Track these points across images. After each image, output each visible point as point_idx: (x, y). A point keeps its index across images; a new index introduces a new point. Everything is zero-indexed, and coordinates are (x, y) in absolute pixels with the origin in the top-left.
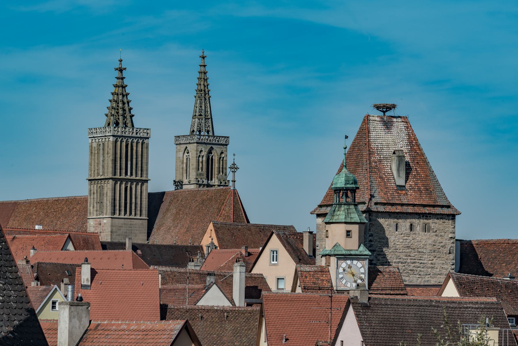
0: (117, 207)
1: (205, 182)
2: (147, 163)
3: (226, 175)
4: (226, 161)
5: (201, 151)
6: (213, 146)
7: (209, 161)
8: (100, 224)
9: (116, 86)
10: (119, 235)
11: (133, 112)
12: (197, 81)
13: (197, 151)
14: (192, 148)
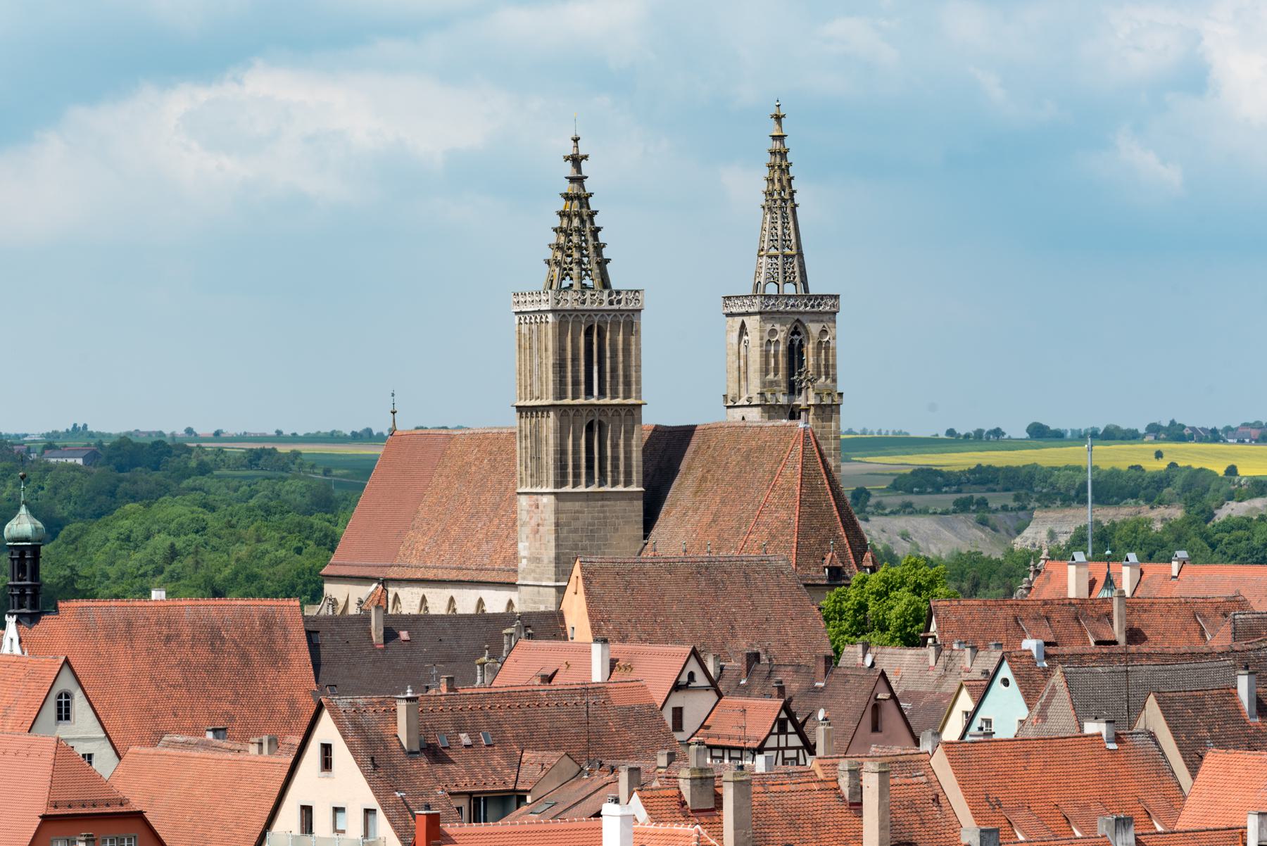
0: (570, 470)
1: (783, 400)
2: (639, 366)
3: (834, 380)
4: (834, 349)
5: (773, 332)
6: (800, 317)
7: (794, 354)
8: (537, 507)
9: (567, 197)
10: (576, 531)
11: (606, 253)
12: (766, 172)
13: (761, 331)
14: (753, 323)
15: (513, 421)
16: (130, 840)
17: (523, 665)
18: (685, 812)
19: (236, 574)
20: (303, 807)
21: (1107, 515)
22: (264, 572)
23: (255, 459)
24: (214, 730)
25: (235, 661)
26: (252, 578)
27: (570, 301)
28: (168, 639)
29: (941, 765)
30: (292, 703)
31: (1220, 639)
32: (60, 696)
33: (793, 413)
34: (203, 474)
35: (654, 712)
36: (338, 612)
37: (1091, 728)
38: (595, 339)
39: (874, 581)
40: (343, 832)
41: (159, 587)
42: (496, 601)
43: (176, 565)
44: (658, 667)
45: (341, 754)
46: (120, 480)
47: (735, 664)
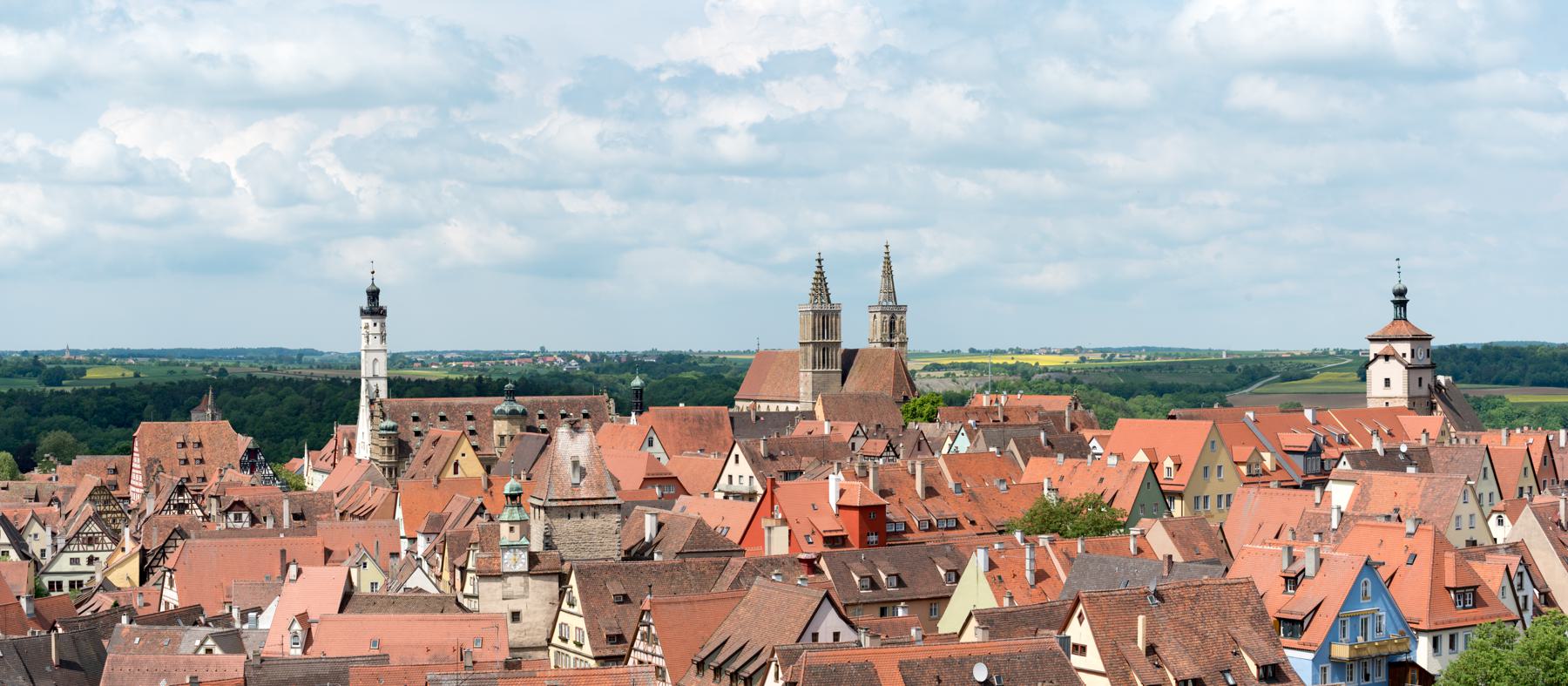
7: (892, 325)
15: (798, 347)
17: (801, 429)
18: (857, 478)
21: (996, 379)
23: (712, 359)
27: (817, 307)
29: (941, 462)
31: (1034, 420)
33: (892, 345)
35: (846, 444)
37: (992, 449)
38: (825, 320)
39: (919, 401)
42: (792, 407)
44: (847, 429)
47: (872, 428)
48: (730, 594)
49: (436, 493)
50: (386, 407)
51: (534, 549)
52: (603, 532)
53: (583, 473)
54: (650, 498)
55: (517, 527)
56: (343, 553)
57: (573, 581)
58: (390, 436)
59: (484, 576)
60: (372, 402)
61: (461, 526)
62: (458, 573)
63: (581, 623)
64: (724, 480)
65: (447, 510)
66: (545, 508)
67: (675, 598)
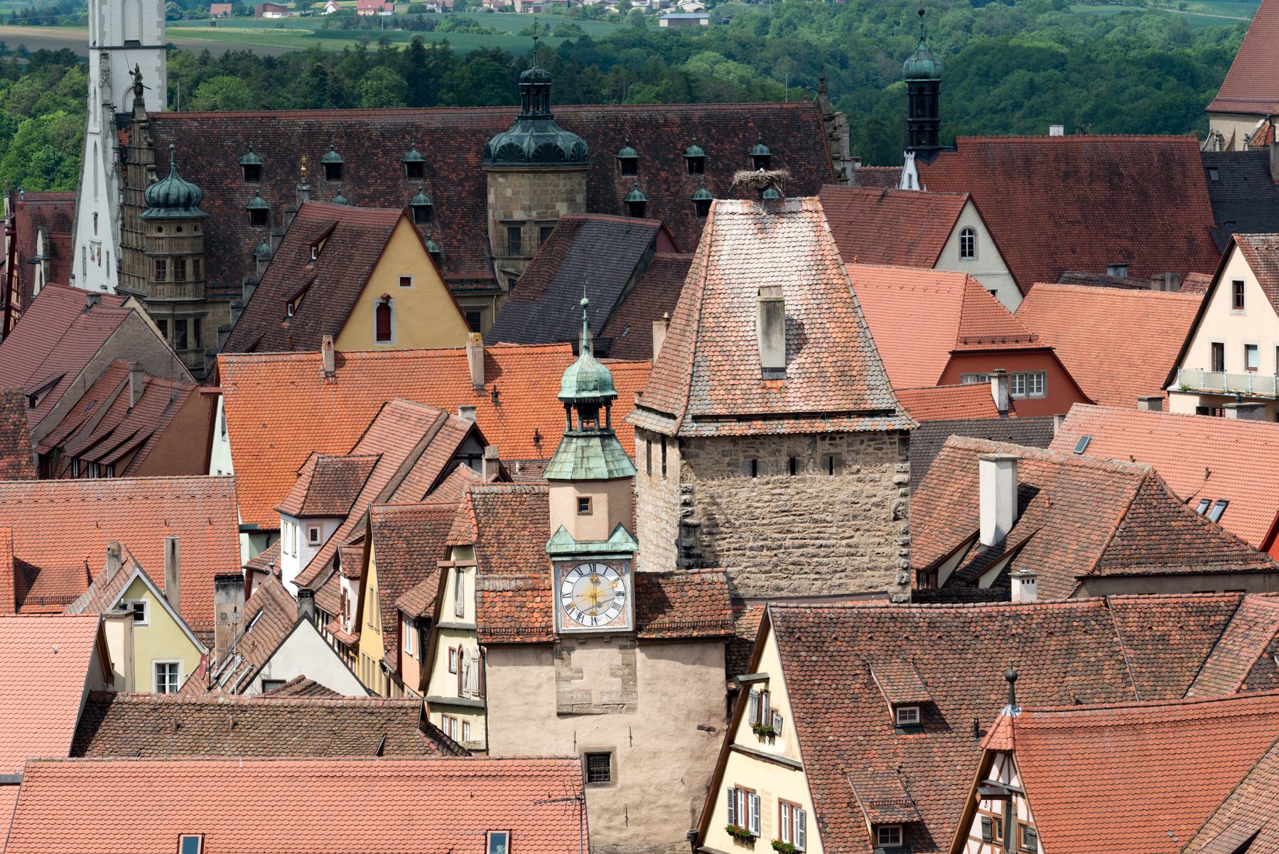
16: (1039, 376)
19: (1096, 109)
20: (1214, 344)
22: (1124, 108)
24: (1116, 267)
25: (1134, 199)
26: (1112, 113)
28: (1067, 175)
30: (1191, 240)
32: (964, 233)
34: (1059, 9)
36: (1225, 149)
40: (1255, 369)
41: (1058, 123)
43: (1034, 100)
45: (1254, 291)
46: (976, 15)
48: (1252, 704)
49: (330, 397)
50: (168, 138)
51: (649, 563)
52: (857, 515)
53: (796, 339)
54: (972, 413)
55: (600, 501)
56: (70, 574)
57: (771, 661)
58: (179, 223)
59: (501, 644)
60: (121, 123)
61: (412, 494)
62: (410, 636)
63: (796, 787)
64: (1200, 356)
65: (367, 449)
66: (682, 442)
67: (1086, 716)
